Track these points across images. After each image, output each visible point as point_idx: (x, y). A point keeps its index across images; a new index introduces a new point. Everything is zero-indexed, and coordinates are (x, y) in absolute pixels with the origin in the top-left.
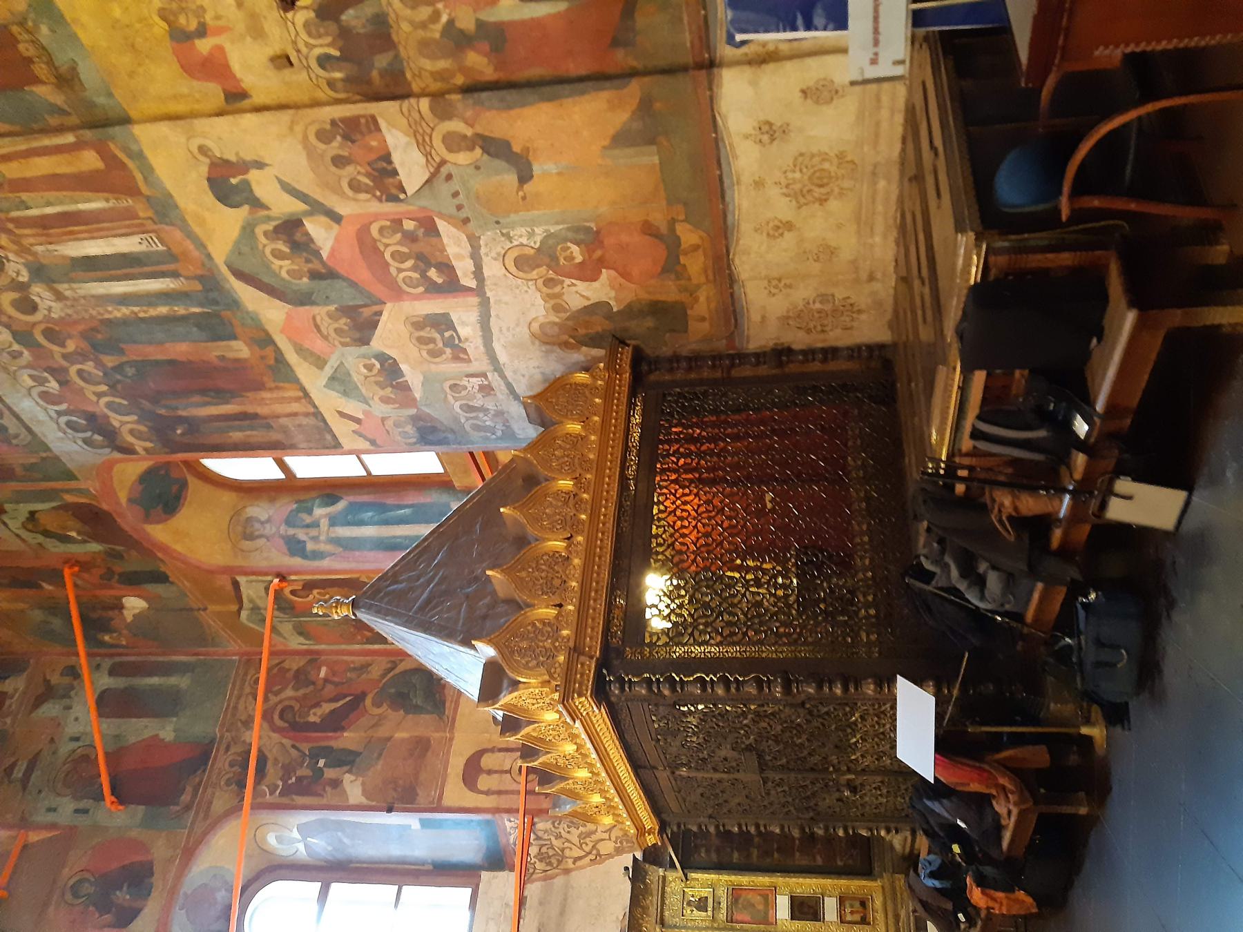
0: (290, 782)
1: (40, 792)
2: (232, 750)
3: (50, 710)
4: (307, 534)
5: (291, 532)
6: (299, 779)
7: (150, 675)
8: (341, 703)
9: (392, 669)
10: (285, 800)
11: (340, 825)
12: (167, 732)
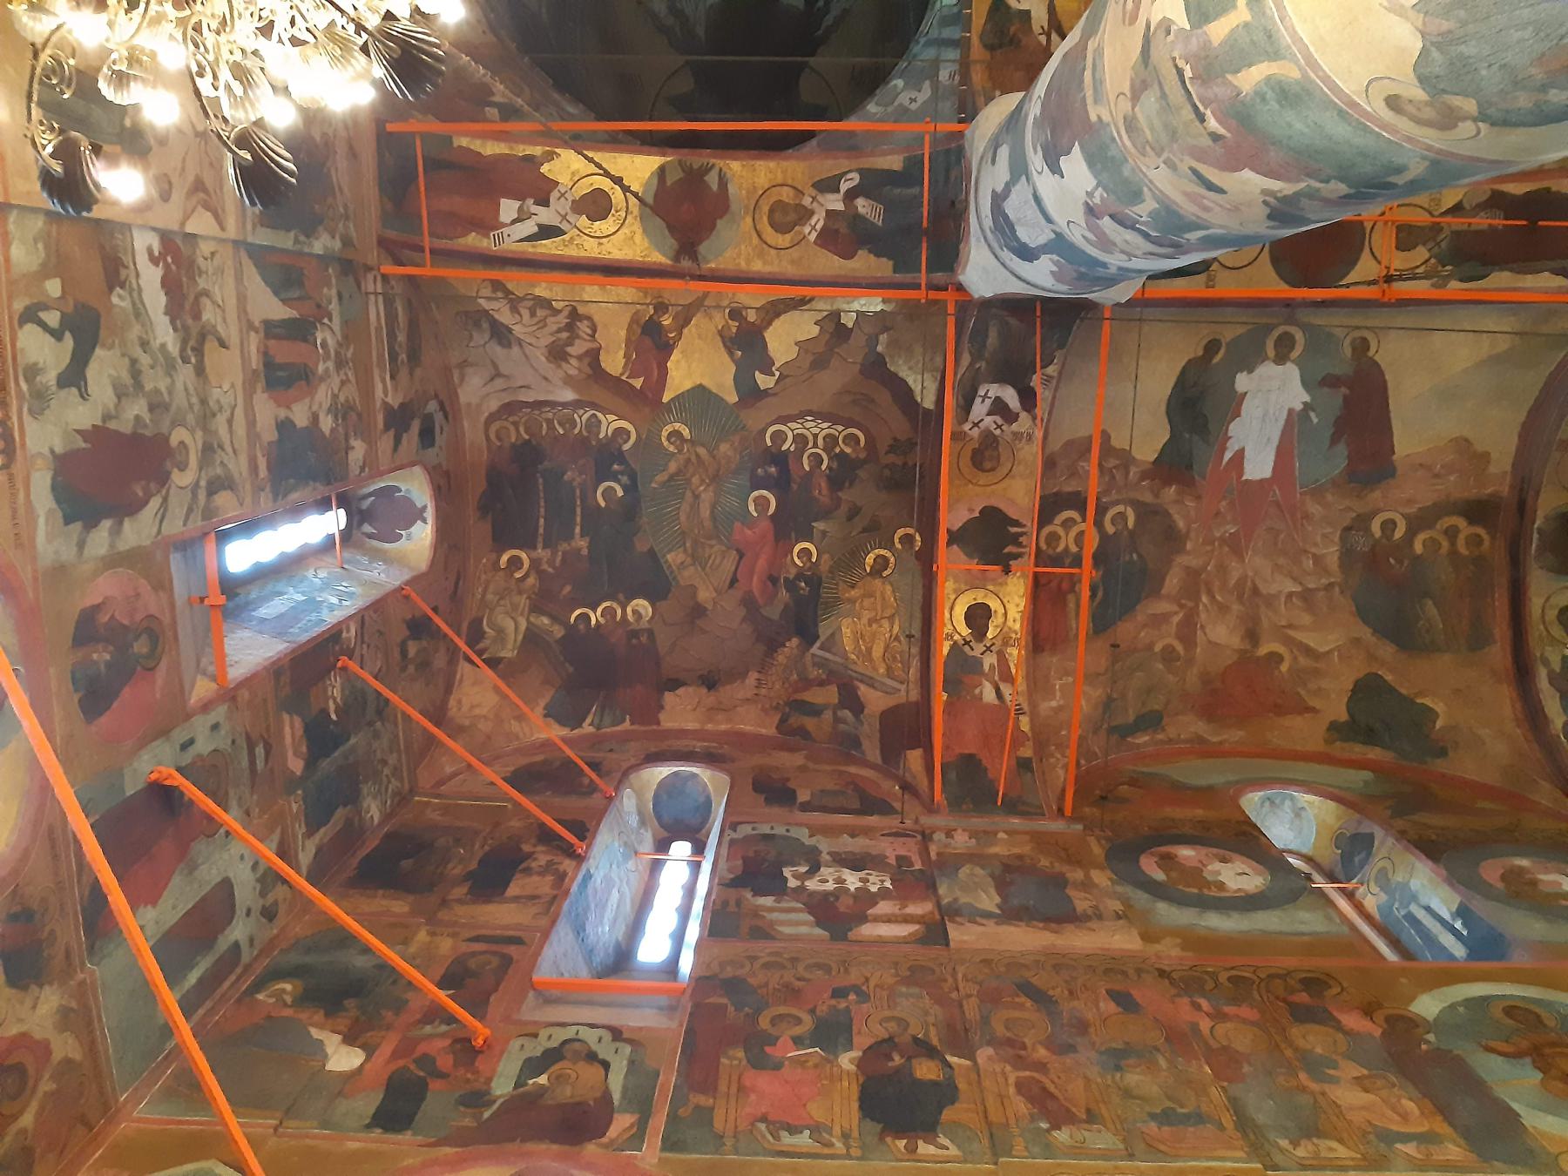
1: (233, 742)
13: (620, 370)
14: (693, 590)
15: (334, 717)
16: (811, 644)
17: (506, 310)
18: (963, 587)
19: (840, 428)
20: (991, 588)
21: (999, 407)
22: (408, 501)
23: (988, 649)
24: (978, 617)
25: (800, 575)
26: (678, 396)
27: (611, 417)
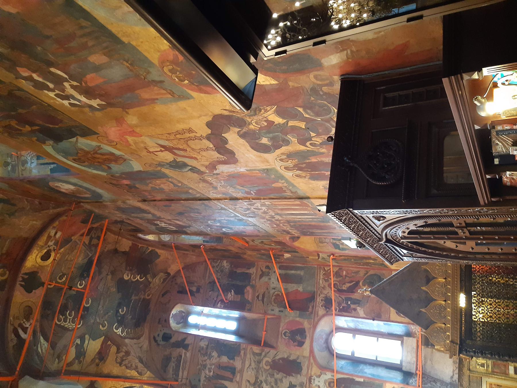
0: (341, 308)
1: (268, 304)
2: (321, 296)
3: (265, 279)
4: (339, 242)
5: (334, 241)
6: (343, 307)
7: (291, 270)
8: (352, 284)
9: (366, 274)
10: (340, 313)
11: (357, 321)
12: (300, 289)
13: (113, 347)
14: (112, 280)
15: (232, 291)
16: (91, 257)
17: (139, 367)
18: (46, 267)
19: (62, 324)
20: (37, 265)
21: (25, 330)
22: (174, 320)
23: (49, 246)
24: (46, 257)
25: (85, 278)
26: (100, 338)
27: (118, 333)
